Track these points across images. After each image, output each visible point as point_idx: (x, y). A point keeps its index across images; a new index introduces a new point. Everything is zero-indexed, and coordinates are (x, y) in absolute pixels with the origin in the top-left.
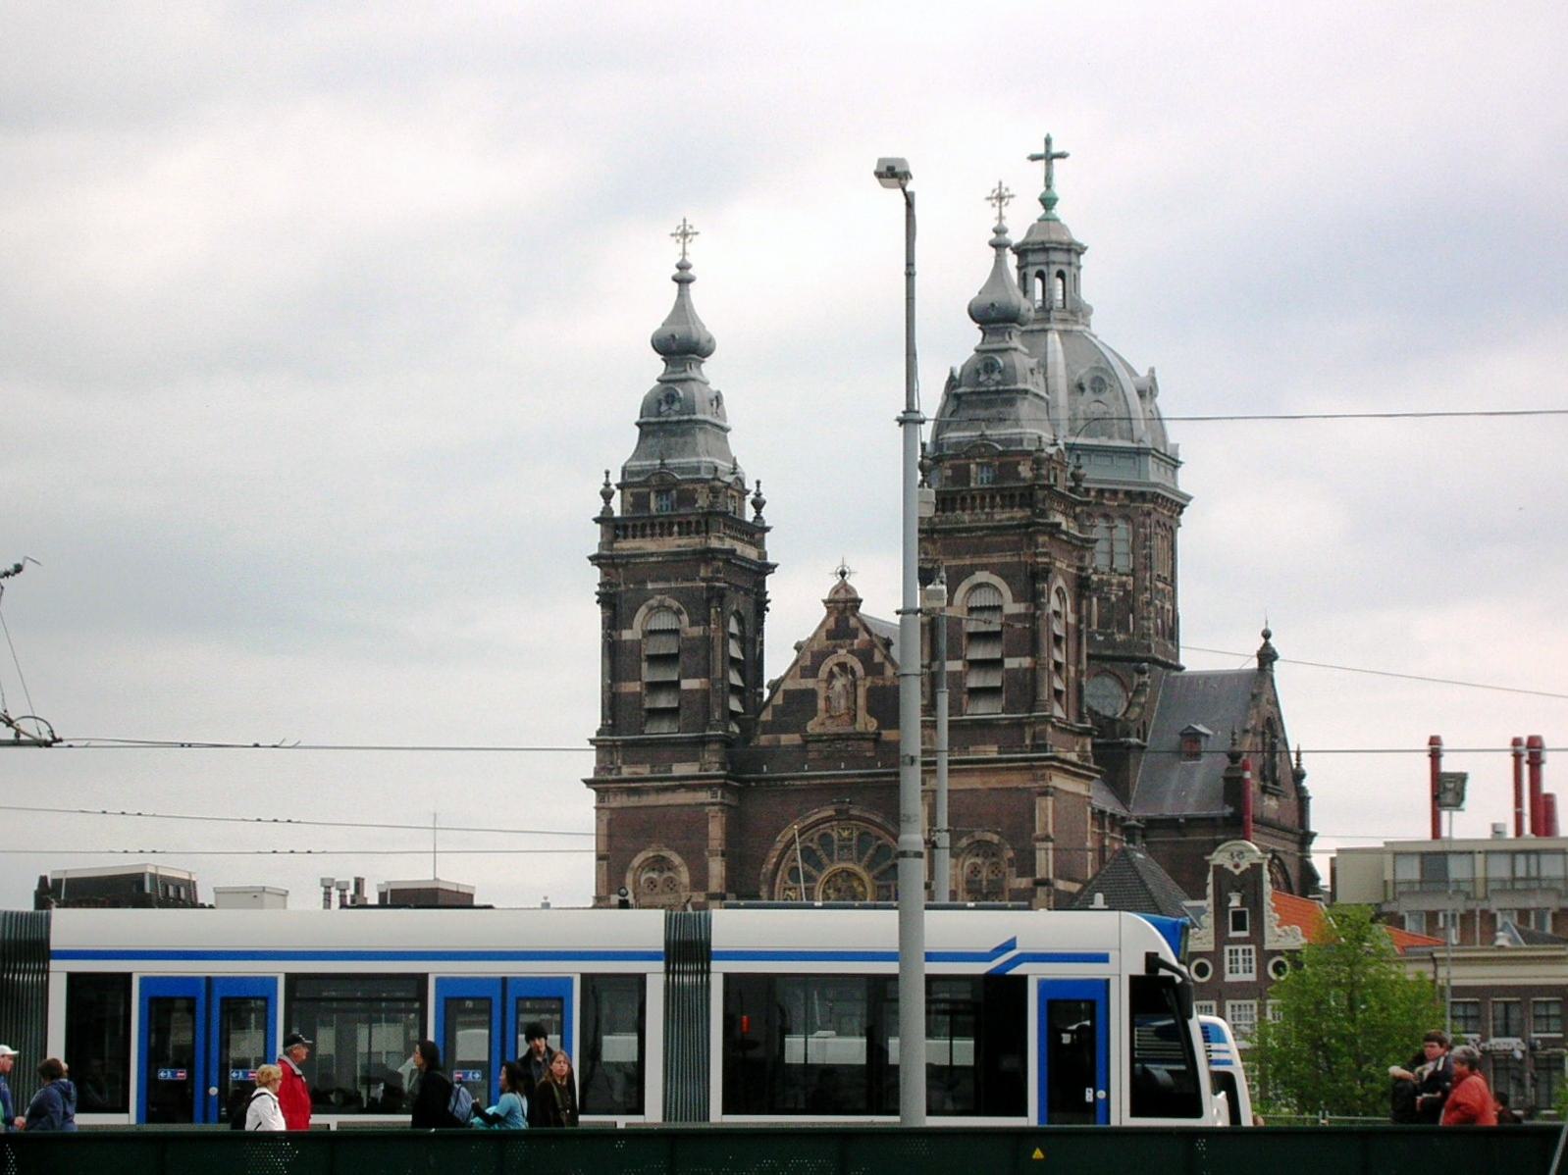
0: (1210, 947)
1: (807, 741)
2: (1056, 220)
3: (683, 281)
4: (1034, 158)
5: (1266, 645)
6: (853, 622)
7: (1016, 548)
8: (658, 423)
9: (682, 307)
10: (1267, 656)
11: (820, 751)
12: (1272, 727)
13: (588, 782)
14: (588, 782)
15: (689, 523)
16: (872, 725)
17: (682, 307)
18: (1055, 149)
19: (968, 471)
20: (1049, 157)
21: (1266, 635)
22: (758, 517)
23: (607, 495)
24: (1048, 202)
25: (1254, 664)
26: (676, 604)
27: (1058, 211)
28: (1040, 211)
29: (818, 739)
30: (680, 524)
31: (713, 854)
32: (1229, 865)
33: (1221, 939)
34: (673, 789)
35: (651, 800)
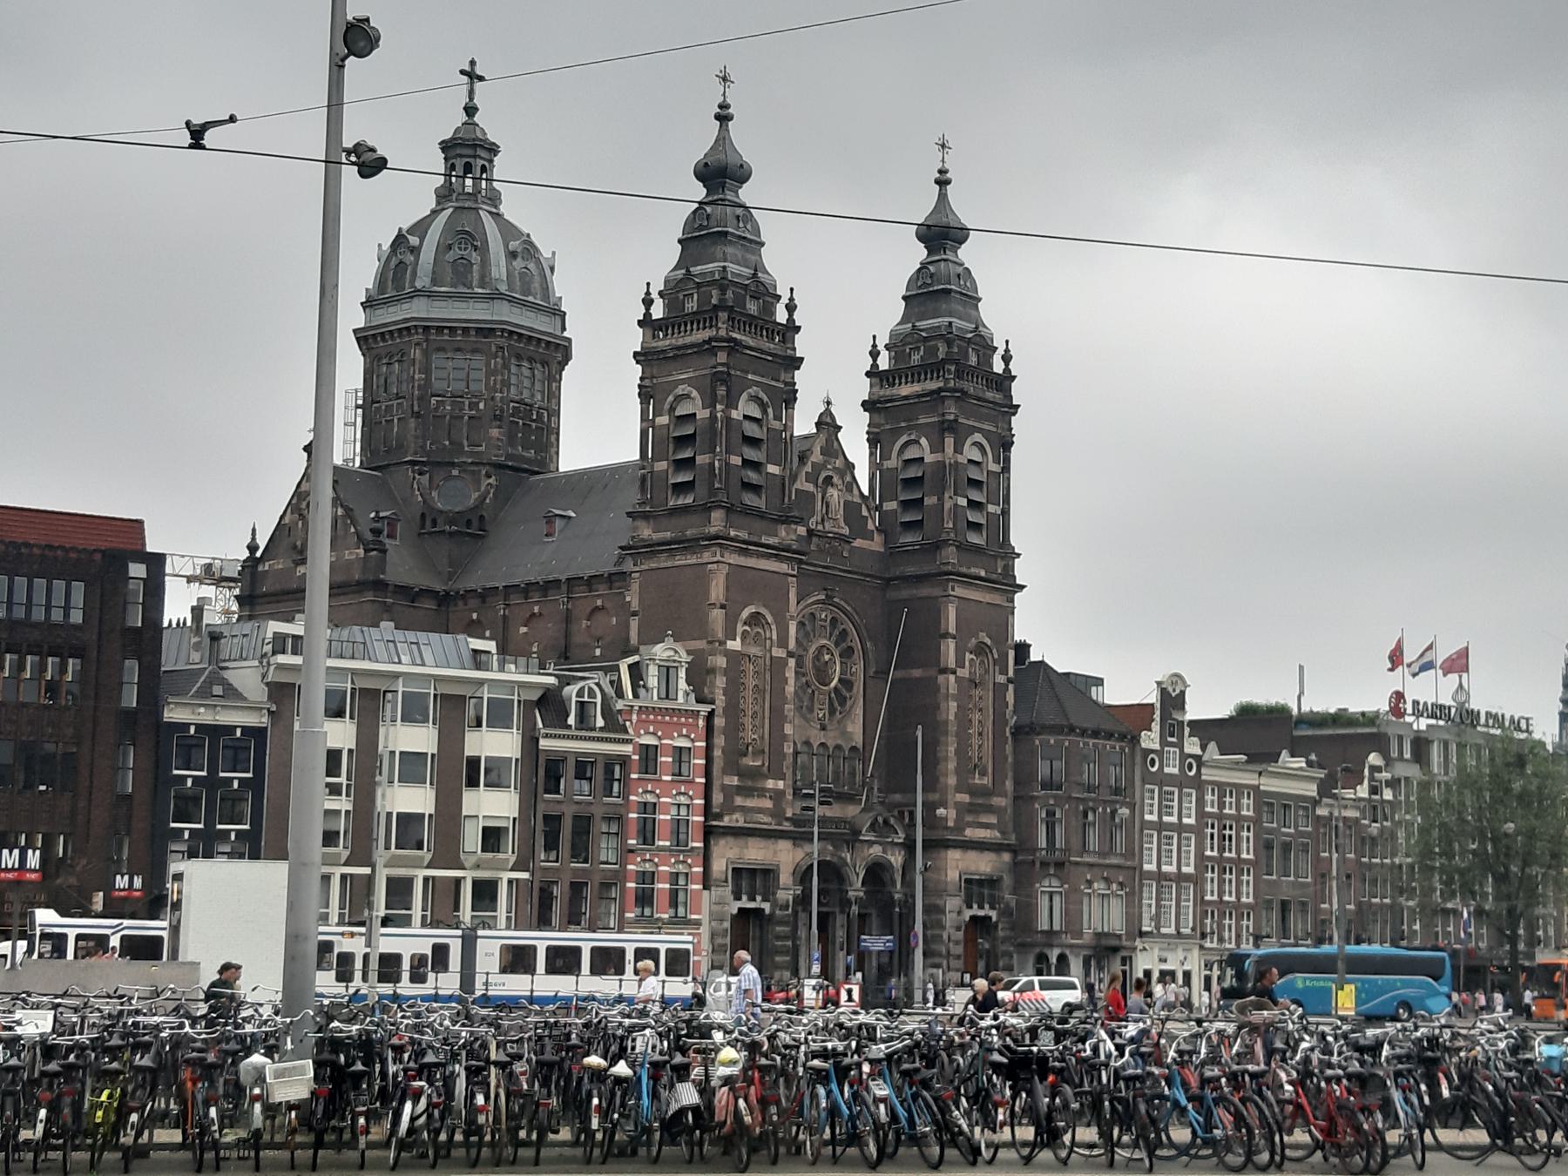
0: (1157, 746)
1: (810, 532)
3: (723, 118)
4: (462, 72)
6: (836, 444)
7: (994, 422)
8: (740, 237)
9: (723, 139)
11: (818, 546)
15: (773, 331)
16: (846, 531)
17: (723, 139)
18: (479, 72)
19: (967, 351)
20: (472, 76)
24: (470, 110)
26: (765, 399)
27: (476, 119)
28: (465, 118)
29: (822, 536)
30: (767, 330)
31: (792, 618)
32: (1170, 689)
33: (1163, 743)
34: (769, 556)
35: (751, 562)
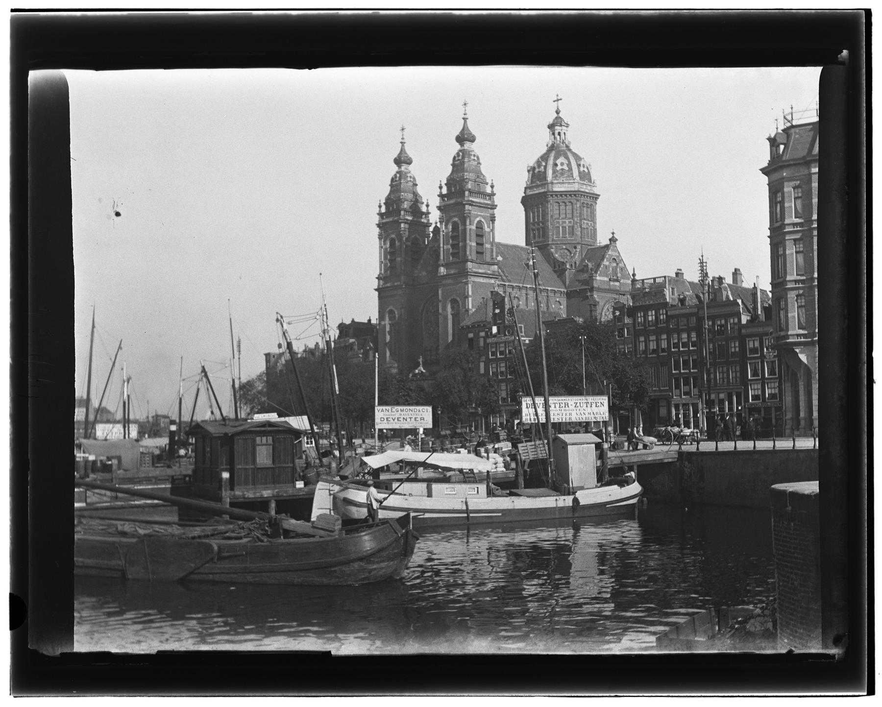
2: (560, 118)
5: (613, 237)
9: (402, 151)
10: (613, 240)
12: (617, 260)
13: (376, 290)
14: (376, 290)
17: (402, 151)
18: (559, 98)
21: (613, 233)
22: (428, 210)
23: (380, 207)
24: (558, 112)
25: (609, 243)
27: (560, 115)
28: (556, 115)
